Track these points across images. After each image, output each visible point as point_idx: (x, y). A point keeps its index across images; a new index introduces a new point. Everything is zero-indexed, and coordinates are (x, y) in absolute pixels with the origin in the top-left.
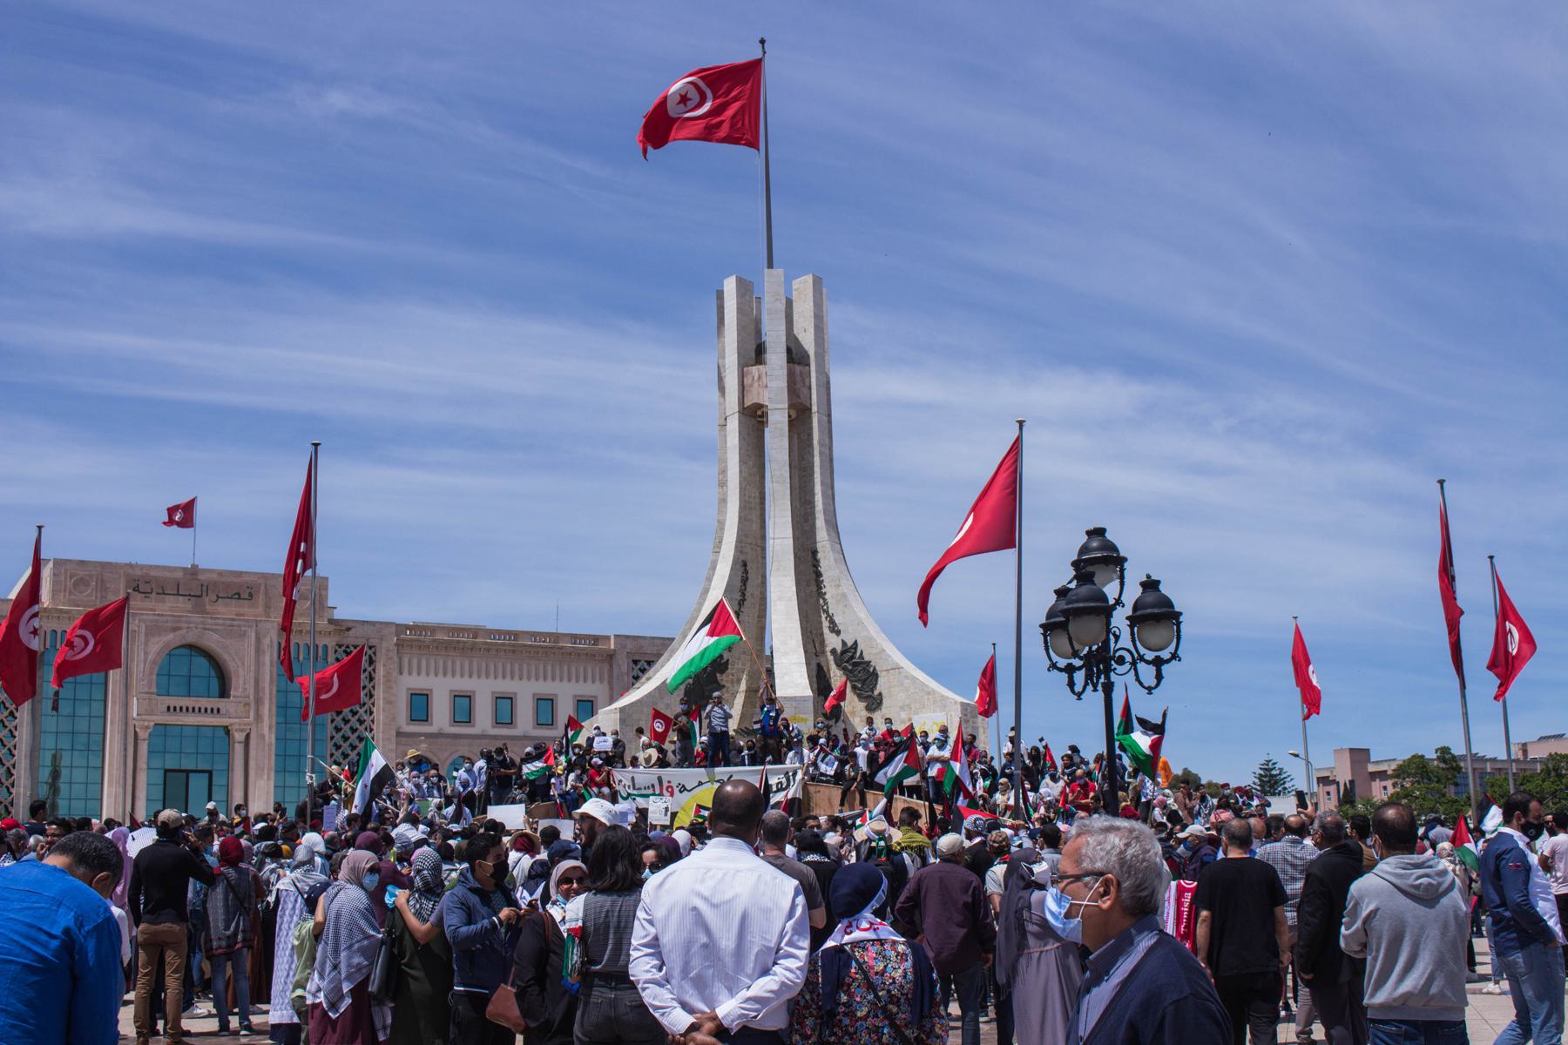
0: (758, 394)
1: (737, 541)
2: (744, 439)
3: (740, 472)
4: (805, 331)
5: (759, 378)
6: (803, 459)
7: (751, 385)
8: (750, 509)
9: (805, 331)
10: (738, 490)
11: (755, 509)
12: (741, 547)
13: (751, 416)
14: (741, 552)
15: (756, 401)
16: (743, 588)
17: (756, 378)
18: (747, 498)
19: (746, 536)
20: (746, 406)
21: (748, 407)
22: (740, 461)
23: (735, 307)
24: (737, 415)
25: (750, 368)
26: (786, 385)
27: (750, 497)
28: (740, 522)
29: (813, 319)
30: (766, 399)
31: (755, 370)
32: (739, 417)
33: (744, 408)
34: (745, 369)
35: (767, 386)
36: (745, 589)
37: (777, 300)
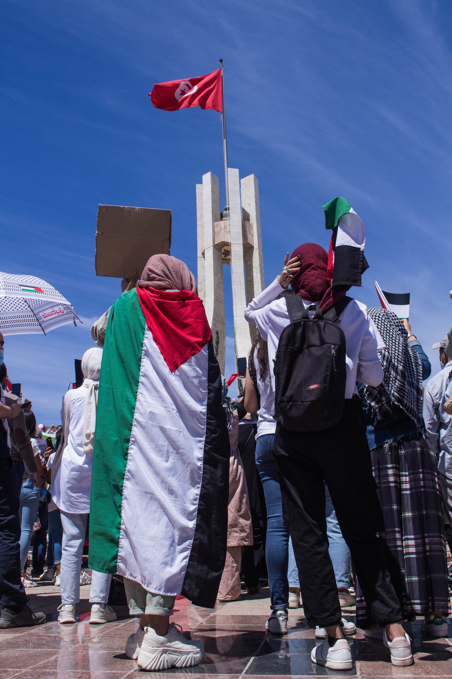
0: (224, 236)
1: (213, 319)
2: (216, 261)
3: (214, 280)
4: (249, 205)
5: (225, 227)
6: (249, 275)
7: (220, 232)
8: (219, 301)
9: (249, 205)
10: (213, 290)
11: (222, 302)
12: (215, 323)
13: (219, 250)
14: (215, 326)
15: (224, 241)
16: (217, 347)
17: (223, 227)
18: (217, 295)
19: (218, 317)
20: (216, 243)
21: (218, 244)
22: (214, 274)
23: (210, 188)
24: (212, 248)
25: (219, 222)
26: (241, 231)
27: (219, 295)
28: (215, 309)
29: (254, 198)
30: (229, 239)
31: (222, 223)
32: (213, 249)
33: (216, 245)
34: (216, 223)
35: (230, 232)
36: (218, 348)
37: (235, 185)
